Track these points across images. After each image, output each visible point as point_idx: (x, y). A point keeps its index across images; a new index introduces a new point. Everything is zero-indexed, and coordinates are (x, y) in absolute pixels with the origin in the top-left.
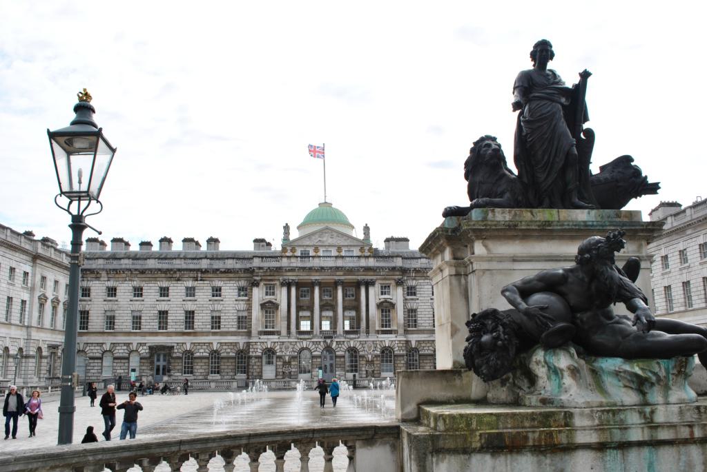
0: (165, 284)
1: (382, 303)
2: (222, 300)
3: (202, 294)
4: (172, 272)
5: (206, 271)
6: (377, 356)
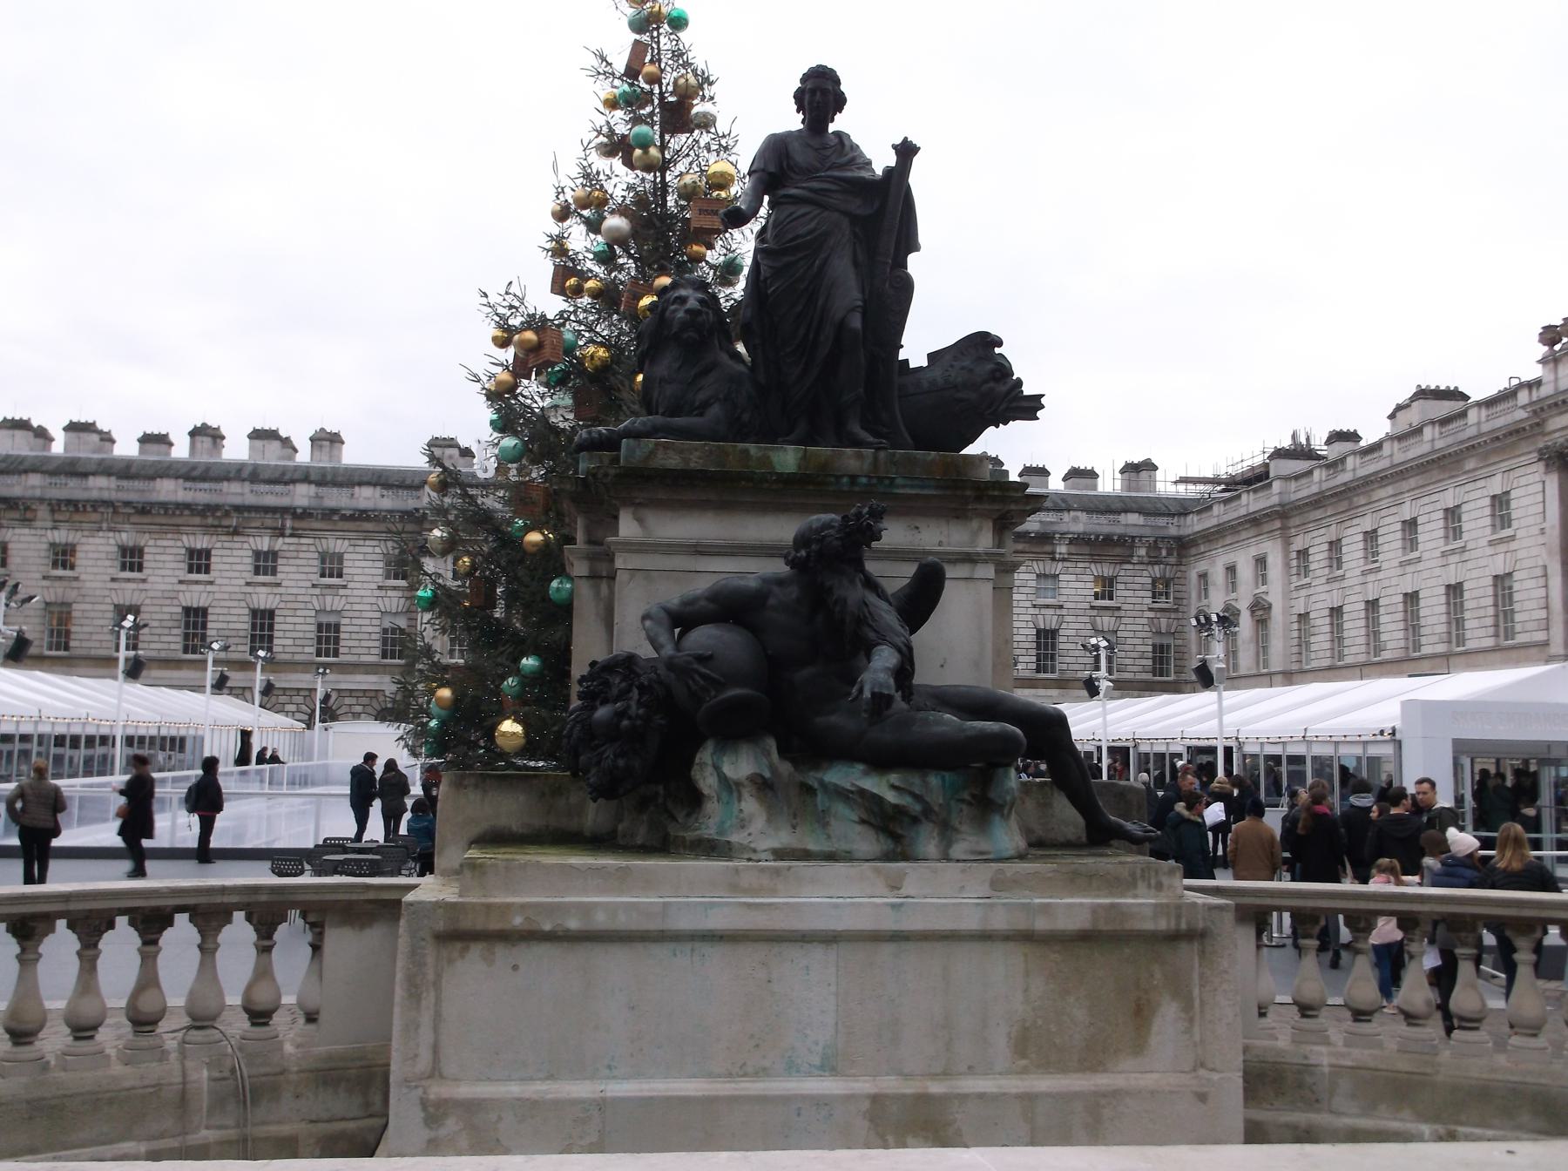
0: (201, 542)
2: (345, 587)
3: (293, 569)
4: (219, 514)
5: (303, 514)
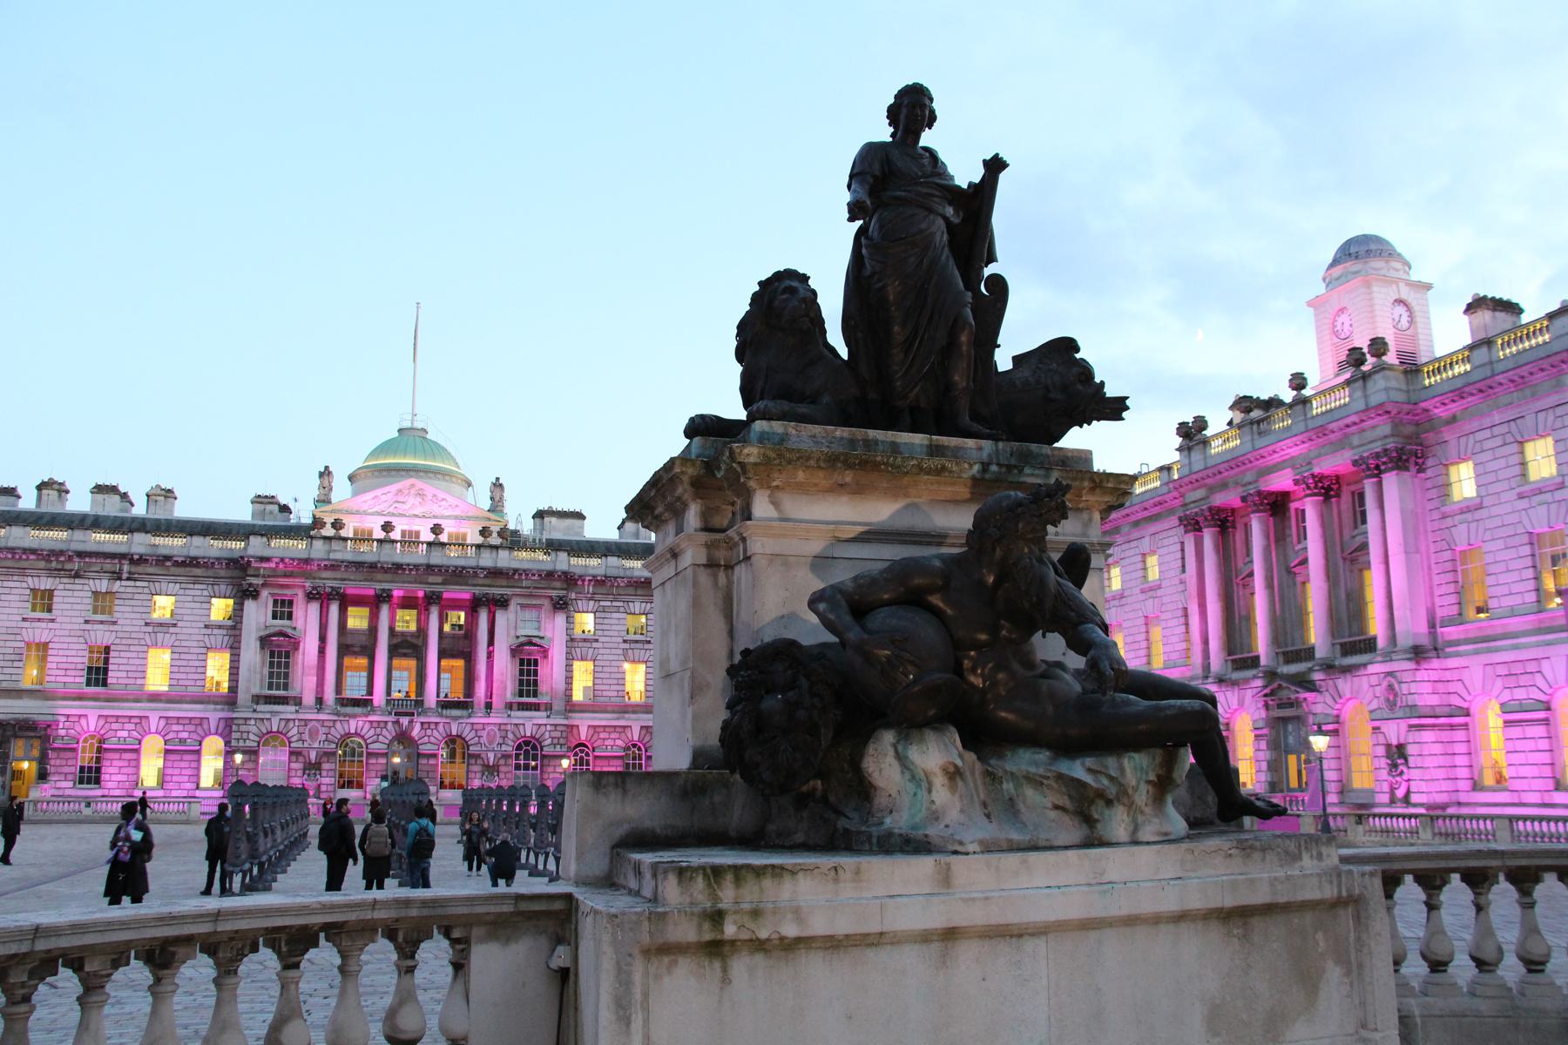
0: (46, 583)
3: (130, 609)
4: (62, 559)
5: (142, 560)
6: (506, 756)
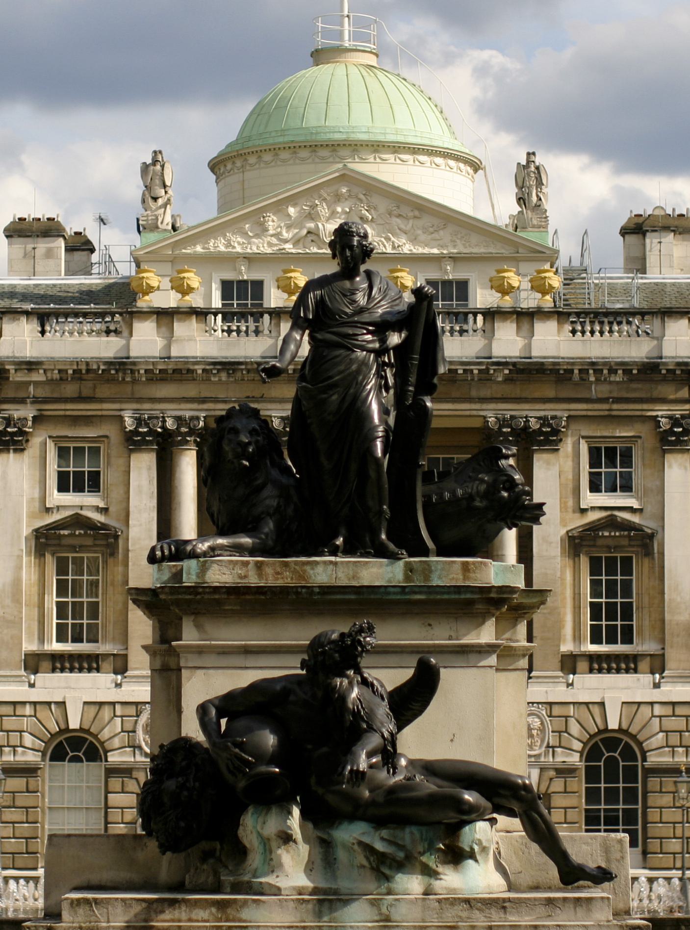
1: (593, 528)
6: (564, 772)
